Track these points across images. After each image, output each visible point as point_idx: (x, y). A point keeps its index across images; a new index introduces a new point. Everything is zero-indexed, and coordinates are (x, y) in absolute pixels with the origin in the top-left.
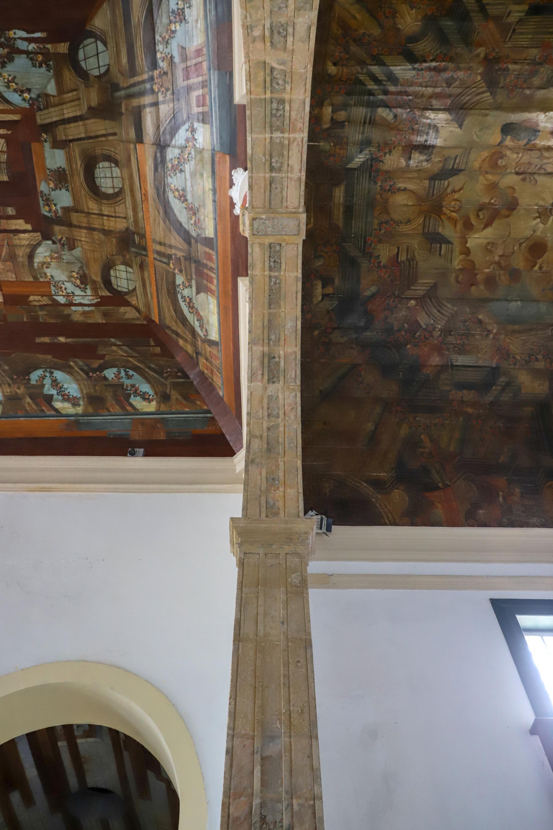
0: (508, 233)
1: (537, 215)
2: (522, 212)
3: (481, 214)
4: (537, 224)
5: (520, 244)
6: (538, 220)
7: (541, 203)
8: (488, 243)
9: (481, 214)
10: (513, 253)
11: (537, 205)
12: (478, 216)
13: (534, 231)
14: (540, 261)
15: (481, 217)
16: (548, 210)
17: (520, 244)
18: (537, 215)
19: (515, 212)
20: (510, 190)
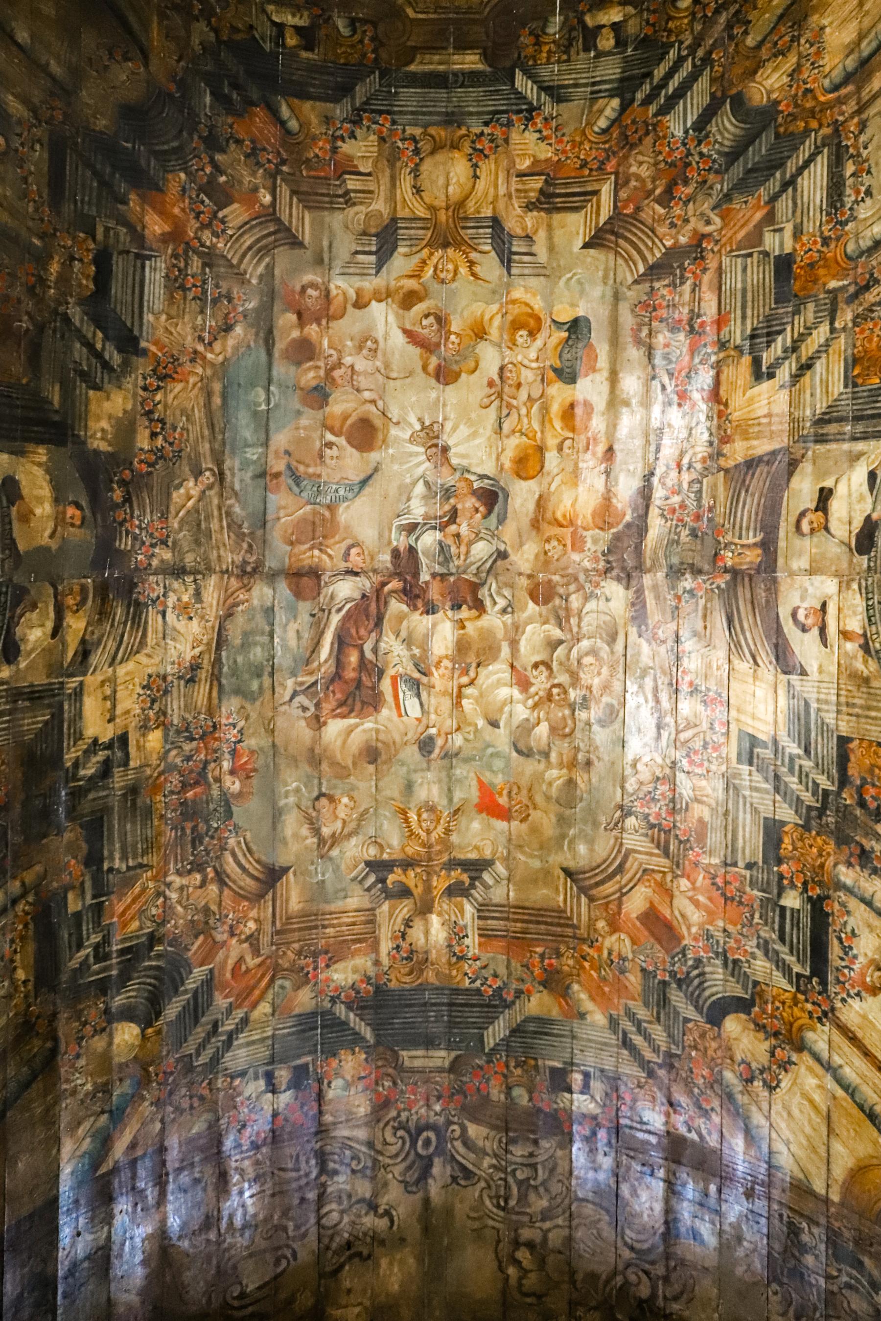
0: (394, 375)
1: (427, 423)
2: (434, 395)
3: (431, 319)
4: (410, 425)
5: (373, 402)
6: (418, 427)
7: (448, 426)
8: (376, 342)
9: (431, 319)
10: (358, 390)
11: (445, 419)
12: (426, 316)
13: (398, 423)
14: (342, 441)
15: (425, 322)
16: (435, 441)
17: (373, 402)
18: (427, 423)
19: (433, 381)
20: (473, 364)
